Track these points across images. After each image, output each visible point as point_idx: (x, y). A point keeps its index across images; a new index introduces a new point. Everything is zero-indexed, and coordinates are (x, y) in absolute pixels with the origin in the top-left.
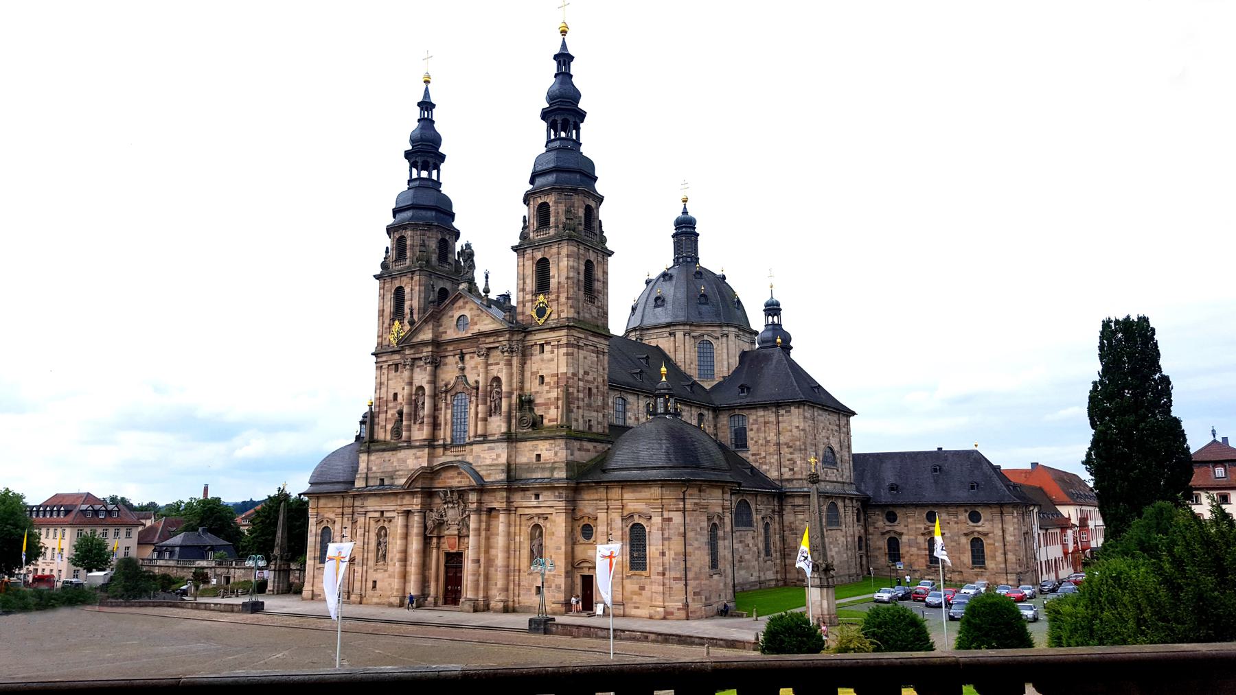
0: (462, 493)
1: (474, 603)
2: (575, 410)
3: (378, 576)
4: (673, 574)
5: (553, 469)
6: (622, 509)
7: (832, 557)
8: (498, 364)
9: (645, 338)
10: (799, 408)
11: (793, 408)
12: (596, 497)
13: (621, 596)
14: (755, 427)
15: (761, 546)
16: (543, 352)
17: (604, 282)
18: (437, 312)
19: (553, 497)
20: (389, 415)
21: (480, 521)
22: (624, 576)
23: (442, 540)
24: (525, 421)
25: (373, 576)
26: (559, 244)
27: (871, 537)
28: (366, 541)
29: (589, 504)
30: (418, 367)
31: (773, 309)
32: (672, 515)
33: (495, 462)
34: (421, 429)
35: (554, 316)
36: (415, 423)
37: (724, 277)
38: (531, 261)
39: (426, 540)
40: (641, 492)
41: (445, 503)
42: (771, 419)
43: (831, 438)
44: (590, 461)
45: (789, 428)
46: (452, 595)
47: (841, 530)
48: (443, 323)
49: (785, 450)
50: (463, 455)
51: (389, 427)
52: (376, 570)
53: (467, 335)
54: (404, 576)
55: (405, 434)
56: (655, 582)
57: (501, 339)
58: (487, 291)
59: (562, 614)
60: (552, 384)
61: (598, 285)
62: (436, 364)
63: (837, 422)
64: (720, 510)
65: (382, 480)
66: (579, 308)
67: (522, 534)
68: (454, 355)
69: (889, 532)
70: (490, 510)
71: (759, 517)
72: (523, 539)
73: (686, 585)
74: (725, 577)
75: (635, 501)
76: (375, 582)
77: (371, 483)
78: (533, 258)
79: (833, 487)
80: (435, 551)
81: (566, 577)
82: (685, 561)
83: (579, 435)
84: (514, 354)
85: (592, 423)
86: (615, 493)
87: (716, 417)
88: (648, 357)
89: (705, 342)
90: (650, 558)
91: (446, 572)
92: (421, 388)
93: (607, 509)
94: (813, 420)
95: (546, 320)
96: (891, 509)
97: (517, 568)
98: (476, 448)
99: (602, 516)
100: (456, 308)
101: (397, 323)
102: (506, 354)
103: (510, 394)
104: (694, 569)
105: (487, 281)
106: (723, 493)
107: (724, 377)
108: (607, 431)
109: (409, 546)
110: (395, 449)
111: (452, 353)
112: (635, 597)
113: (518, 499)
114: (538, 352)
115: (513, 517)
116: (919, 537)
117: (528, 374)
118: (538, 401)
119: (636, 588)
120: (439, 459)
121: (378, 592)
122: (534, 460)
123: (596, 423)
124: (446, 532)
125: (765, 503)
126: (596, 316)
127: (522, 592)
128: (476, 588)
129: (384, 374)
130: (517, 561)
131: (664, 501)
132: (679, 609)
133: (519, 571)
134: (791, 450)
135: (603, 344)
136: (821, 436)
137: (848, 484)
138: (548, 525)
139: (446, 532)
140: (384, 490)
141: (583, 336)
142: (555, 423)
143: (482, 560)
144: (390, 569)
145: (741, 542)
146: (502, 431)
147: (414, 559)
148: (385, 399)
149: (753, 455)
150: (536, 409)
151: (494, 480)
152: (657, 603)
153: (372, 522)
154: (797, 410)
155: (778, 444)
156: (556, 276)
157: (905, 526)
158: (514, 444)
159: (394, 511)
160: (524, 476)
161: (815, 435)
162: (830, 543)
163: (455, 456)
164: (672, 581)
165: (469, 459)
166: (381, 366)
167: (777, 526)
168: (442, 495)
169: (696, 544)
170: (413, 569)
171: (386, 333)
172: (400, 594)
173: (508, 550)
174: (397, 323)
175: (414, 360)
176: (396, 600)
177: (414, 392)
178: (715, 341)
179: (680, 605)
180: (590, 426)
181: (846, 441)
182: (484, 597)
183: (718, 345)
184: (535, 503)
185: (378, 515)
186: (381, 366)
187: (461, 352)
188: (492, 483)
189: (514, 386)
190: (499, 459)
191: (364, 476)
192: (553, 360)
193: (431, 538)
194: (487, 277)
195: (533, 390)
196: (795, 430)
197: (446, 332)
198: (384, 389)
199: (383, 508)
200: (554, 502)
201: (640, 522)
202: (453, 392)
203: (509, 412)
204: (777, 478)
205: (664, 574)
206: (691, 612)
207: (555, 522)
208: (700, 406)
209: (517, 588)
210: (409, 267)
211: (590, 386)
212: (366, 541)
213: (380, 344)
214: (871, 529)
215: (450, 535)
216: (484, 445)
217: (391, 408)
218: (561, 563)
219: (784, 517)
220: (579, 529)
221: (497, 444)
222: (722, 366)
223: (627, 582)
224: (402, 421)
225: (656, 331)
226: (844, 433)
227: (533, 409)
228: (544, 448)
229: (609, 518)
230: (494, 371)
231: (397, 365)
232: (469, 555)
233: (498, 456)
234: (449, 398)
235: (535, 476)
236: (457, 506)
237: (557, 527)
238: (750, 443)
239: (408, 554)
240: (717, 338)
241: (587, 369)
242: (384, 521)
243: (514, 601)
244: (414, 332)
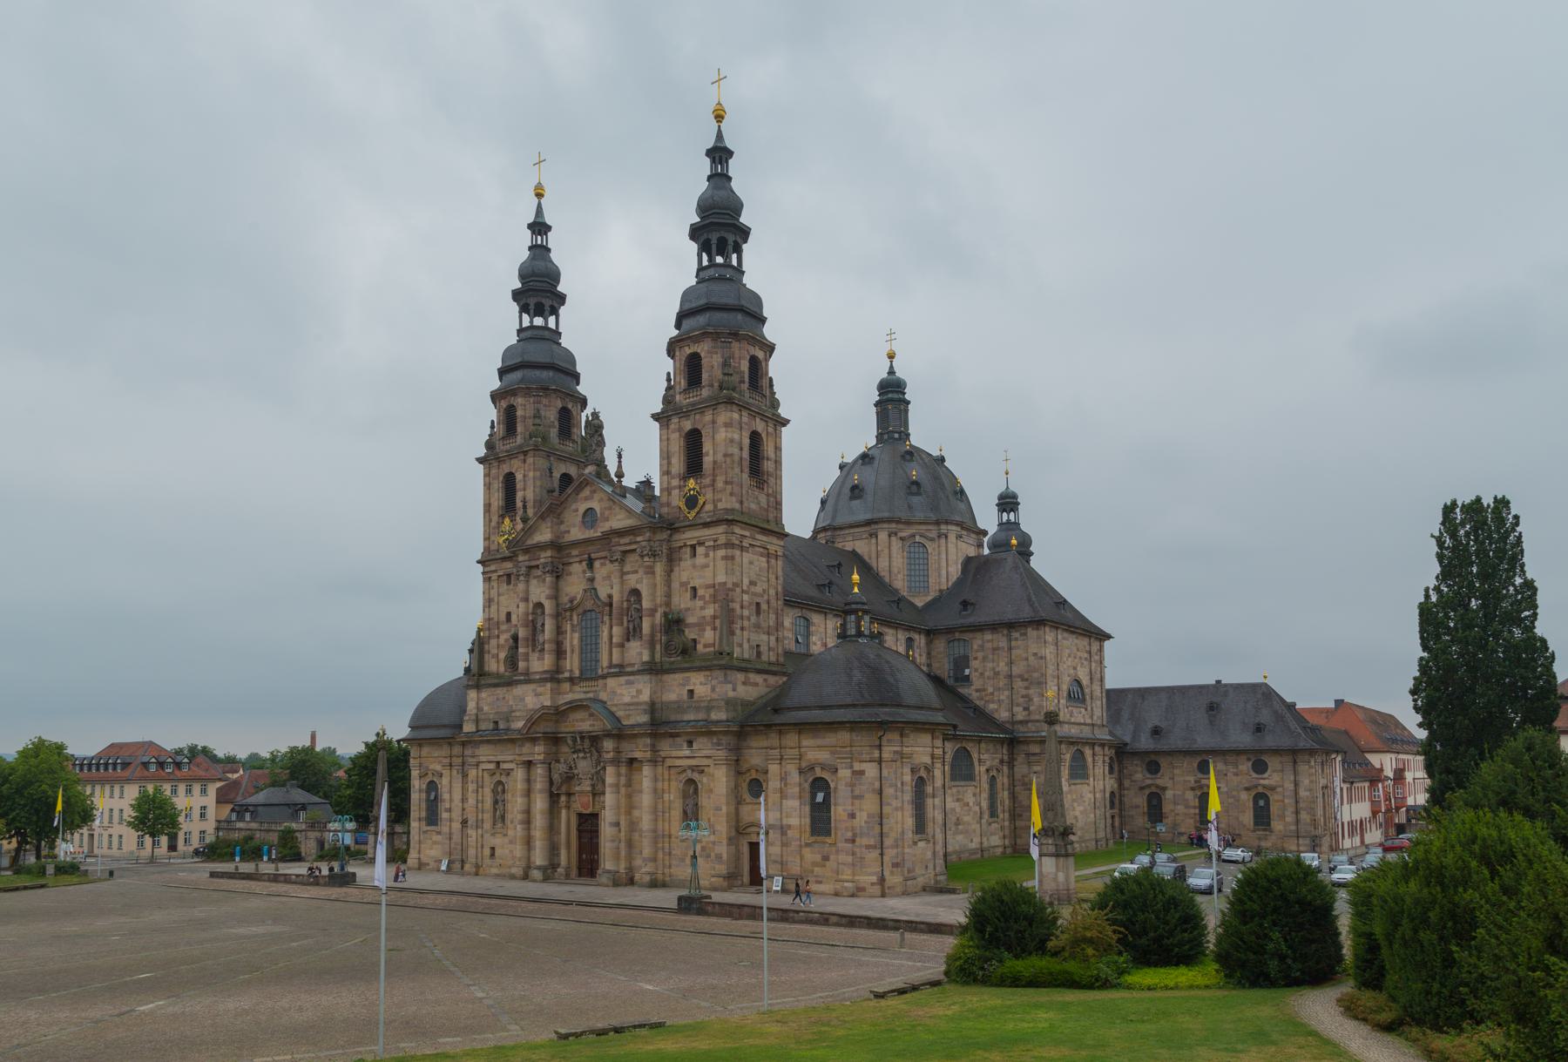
0: (595, 740)
1: (614, 876)
2: (738, 632)
3: (497, 841)
4: (865, 841)
5: (709, 709)
6: (800, 759)
7: (1076, 817)
8: (636, 572)
9: (838, 540)
10: (1038, 629)
11: (1029, 630)
12: (765, 743)
13: (799, 868)
14: (980, 655)
15: (985, 804)
16: (695, 555)
17: (776, 462)
18: (557, 505)
19: (710, 745)
21: (619, 775)
22: (803, 843)
23: (573, 798)
24: (673, 647)
25: (491, 841)
26: (714, 409)
27: (1126, 792)
28: (480, 798)
29: (756, 753)
30: (535, 577)
31: (1008, 502)
32: (864, 766)
33: (636, 700)
34: (541, 659)
35: (709, 507)
36: (533, 651)
37: (942, 459)
38: (678, 434)
39: (553, 798)
40: (824, 738)
41: (574, 753)
42: (1001, 645)
43: (1078, 668)
44: (758, 699)
45: (1024, 655)
46: (588, 866)
47: (1088, 784)
48: (565, 520)
49: (1019, 684)
50: (596, 691)
51: (502, 655)
52: (493, 835)
53: (596, 535)
54: (528, 842)
55: (521, 665)
56: (842, 851)
57: (639, 539)
58: (620, 475)
59: (724, 890)
60: (707, 598)
61: (768, 466)
62: (558, 573)
63: (1088, 648)
64: (927, 760)
65: (496, 723)
66: (742, 496)
67: (672, 790)
68: (580, 562)
69: (1149, 786)
70: (632, 761)
71: (983, 769)
72: (673, 797)
73: (882, 854)
74: (934, 843)
75: (816, 750)
76: (493, 849)
77: (483, 726)
78: (680, 429)
79: (1079, 731)
80: (564, 812)
81: (728, 845)
82: (881, 824)
83: (743, 665)
84: (657, 559)
85: (762, 649)
86: (791, 739)
87: (929, 643)
88: (840, 564)
89: (916, 545)
90: (835, 820)
91: (580, 838)
92: (539, 605)
93: (781, 759)
94: (1057, 644)
95: (698, 513)
96: (1153, 757)
97: (666, 833)
98: (611, 682)
99: (774, 768)
101: (507, 521)
102: (646, 559)
103: (653, 611)
104: (893, 835)
105: (620, 462)
106: (933, 739)
107: (941, 591)
108: (781, 659)
109: (532, 805)
110: (510, 683)
111: (578, 559)
112: (816, 869)
113: (665, 747)
114: (688, 556)
115: (660, 768)
116: (1187, 792)
117: (675, 585)
118: (691, 620)
119: (818, 858)
120: (565, 696)
121: (498, 861)
122: (685, 697)
123: (767, 648)
124: (577, 788)
125: (991, 751)
126: (766, 507)
127: (674, 862)
128: (617, 858)
129: (493, 588)
130: (667, 824)
131: (854, 749)
132: (872, 884)
133: (670, 836)
134: (1026, 684)
135: (775, 545)
136: (1065, 666)
137: (1099, 726)
138: (705, 780)
139: (577, 788)
140: (498, 735)
141: (747, 534)
142: (712, 649)
143: (623, 823)
144: (510, 833)
145: (958, 800)
146: (644, 660)
147: (539, 821)
148: (496, 620)
149: (977, 691)
150: (687, 631)
151: (635, 723)
152: (845, 877)
153: (485, 774)
154: (1035, 633)
155: (1010, 676)
156: (711, 452)
157: (1170, 778)
158: (659, 676)
159: (512, 761)
160: (673, 718)
161: (1058, 664)
162: (1074, 801)
163: (585, 692)
164: (864, 850)
165: (603, 696)
166: (490, 578)
167: (1006, 780)
168: (570, 742)
169: (894, 803)
170: (538, 833)
171: (494, 534)
172: (523, 864)
173: (655, 810)
174: (507, 521)
175: (530, 568)
176: (516, 871)
177: (530, 611)
178: (930, 543)
179: (874, 879)
180: (759, 654)
181: (1098, 672)
182: (626, 869)
183: (934, 549)
184: (687, 753)
185: (492, 766)
186: (490, 578)
187: (589, 557)
188: (633, 726)
189: (658, 601)
190: (641, 696)
191: (474, 717)
192: (707, 566)
193: (558, 795)
194: (620, 456)
195: (682, 606)
196: (1031, 658)
197: (569, 532)
198: (494, 608)
199: (499, 758)
200: (710, 752)
201: (823, 776)
202: (580, 610)
203: (652, 635)
204: (1007, 719)
205: (853, 841)
206: (889, 888)
207: (713, 776)
208: (909, 629)
209: (667, 857)
211: (758, 601)
212: (480, 798)
213: (487, 549)
214: (1127, 783)
215: (582, 792)
216: (621, 678)
217: (503, 632)
218: (722, 828)
219: (1016, 769)
220: (745, 786)
221: (637, 677)
222: (940, 576)
223: (807, 852)
224: (517, 648)
225: (852, 531)
226: (1096, 662)
227: (683, 631)
228: (698, 682)
229: (783, 771)
230: (632, 581)
231: (509, 576)
232: (608, 816)
233: (639, 692)
234: (575, 617)
235: (687, 717)
236: (588, 755)
237: (718, 782)
238: (974, 677)
239: (531, 814)
240: (932, 540)
241: (754, 578)
242: (501, 774)
243: (663, 874)
244: (528, 531)
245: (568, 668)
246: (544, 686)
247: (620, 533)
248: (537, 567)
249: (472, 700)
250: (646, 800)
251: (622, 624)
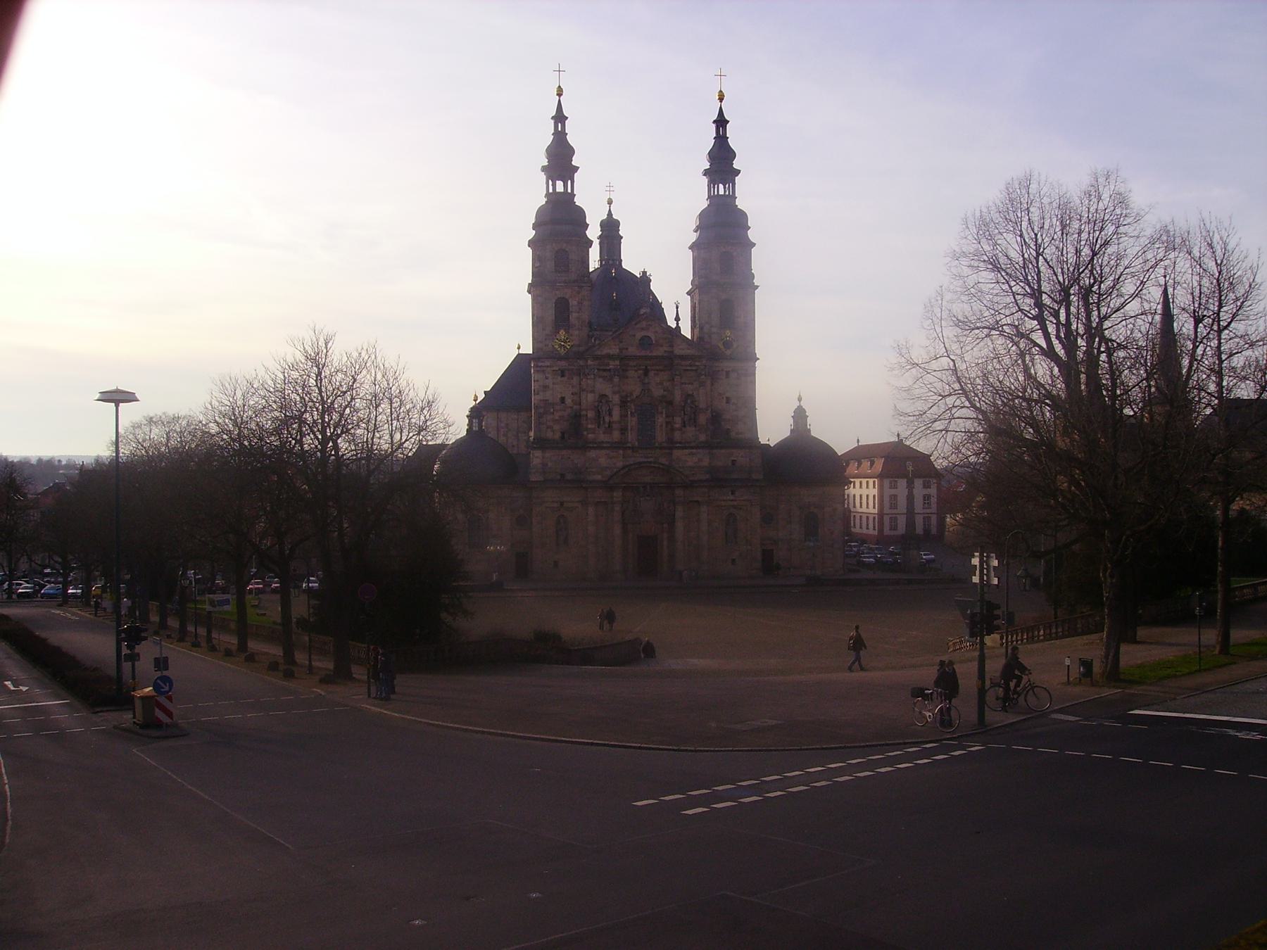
30: (600, 377)
36: (598, 427)
51: (556, 427)
53: (650, 355)
65: (563, 475)
98: (677, 453)
101: (562, 332)
105: (677, 311)
122: (730, 464)
150: (723, 423)
174: (562, 332)
184: (732, 498)
186: (543, 371)
194: (677, 308)
197: (627, 349)
210: (574, 282)
216: (685, 450)
245: (630, 441)
247: (682, 357)
248: (604, 370)
249: (537, 457)
251: (680, 416)
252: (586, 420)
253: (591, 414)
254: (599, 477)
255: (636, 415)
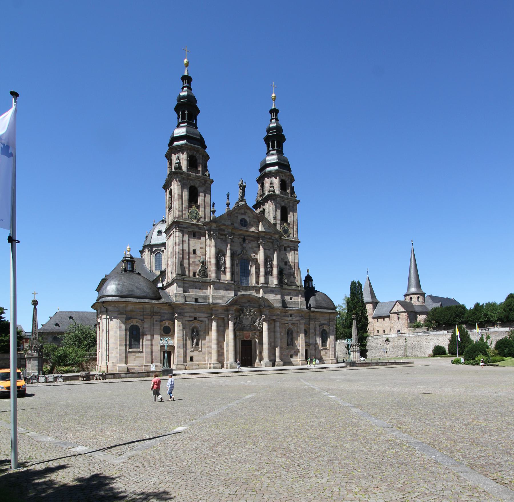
3: (195, 354)
12: (308, 317)
20: (191, 260)
25: (192, 354)
30: (219, 238)
36: (218, 270)
55: (212, 275)
65: (196, 300)
99: (312, 326)
100: (240, 213)
124: (244, 330)
153: (187, 323)
184: (290, 318)
199: (198, 315)
221: (275, 289)
242: (197, 323)
246: (230, 286)
248: (222, 235)
250: (278, 335)
252: (211, 264)
253: (213, 261)
254: (220, 301)
255: (239, 265)
